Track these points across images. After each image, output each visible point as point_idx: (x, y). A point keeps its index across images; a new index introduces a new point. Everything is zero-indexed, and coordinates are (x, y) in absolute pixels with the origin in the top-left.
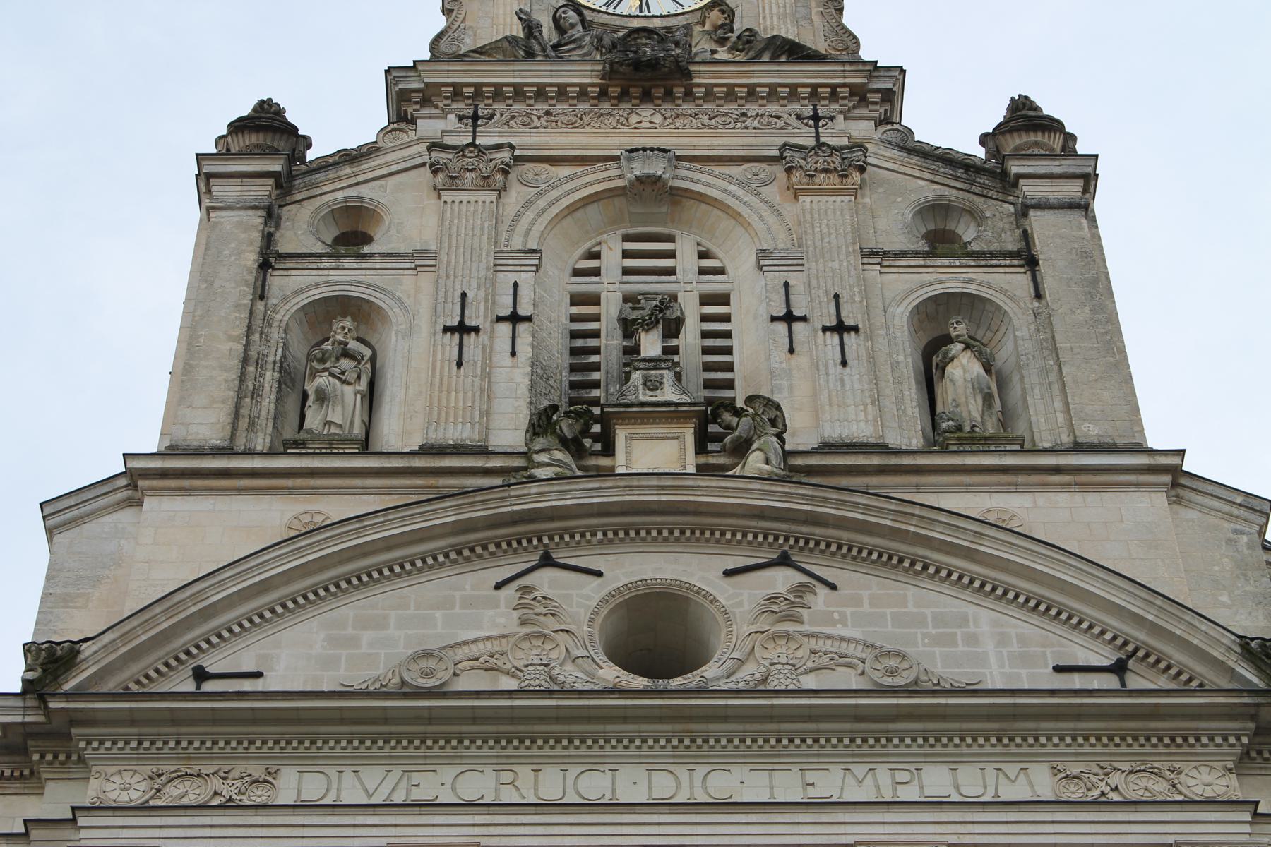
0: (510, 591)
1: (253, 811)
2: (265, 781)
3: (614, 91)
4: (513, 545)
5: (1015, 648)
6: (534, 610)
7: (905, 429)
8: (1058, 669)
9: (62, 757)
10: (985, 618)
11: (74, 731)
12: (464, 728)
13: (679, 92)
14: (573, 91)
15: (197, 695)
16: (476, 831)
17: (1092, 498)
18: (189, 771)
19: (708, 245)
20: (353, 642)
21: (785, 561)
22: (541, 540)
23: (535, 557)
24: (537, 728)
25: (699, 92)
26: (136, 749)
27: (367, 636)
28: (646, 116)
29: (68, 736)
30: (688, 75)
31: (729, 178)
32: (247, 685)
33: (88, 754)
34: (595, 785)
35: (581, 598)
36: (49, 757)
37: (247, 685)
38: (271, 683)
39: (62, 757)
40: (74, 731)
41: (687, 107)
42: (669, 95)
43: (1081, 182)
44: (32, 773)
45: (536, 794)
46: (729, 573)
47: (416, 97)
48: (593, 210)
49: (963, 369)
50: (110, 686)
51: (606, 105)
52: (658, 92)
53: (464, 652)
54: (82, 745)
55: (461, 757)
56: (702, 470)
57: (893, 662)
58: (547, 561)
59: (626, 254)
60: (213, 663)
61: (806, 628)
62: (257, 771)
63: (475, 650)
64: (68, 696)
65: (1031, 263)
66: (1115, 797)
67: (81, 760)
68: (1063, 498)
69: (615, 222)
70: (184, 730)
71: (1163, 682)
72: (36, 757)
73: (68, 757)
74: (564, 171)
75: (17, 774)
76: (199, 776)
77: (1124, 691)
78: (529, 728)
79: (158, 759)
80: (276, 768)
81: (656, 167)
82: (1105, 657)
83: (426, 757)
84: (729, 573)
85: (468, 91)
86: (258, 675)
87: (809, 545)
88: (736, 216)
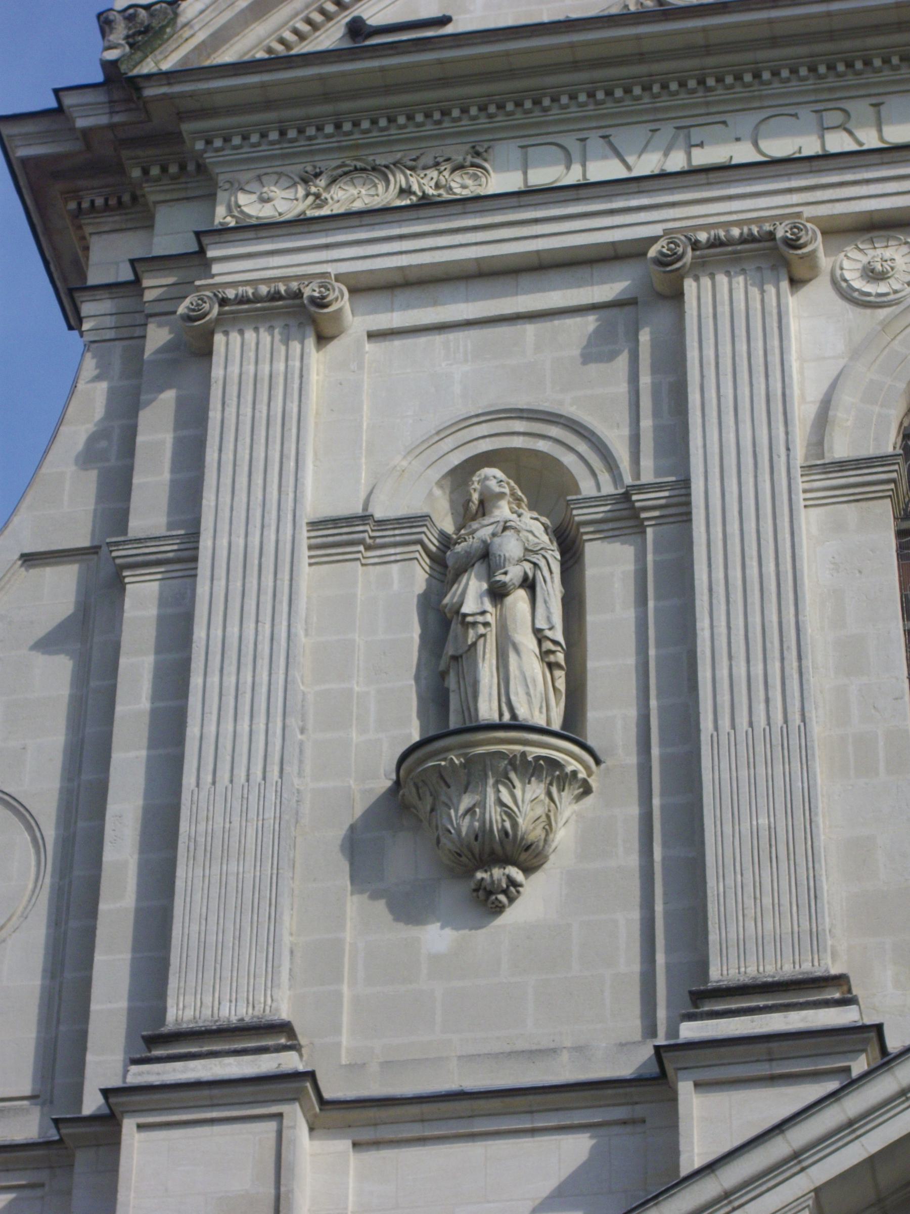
1: (458, 208)
2: (473, 165)
9: (173, 169)
11: (187, 127)
12: (761, 55)
16: (795, 198)
18: (359, 164)
24: (871, 42)
26: (278, 142)
29: (175, 138)
33: (210, 158)
36: (155, 171)
38: (461, 25)
39: (173, 169)
40: (187, 127)
44: (134, 199)
45: (882, 139)
50: (228, 55)
54: (200, 145)
55: (761, 98)
64: (168, 77)
67: (201, 168)
70: (345, 106)
72: (136, 173)
73: (183, 167)
75: (113, 202)
76: (374, 169)
78: (857, 43)
79: (311, 153)
80: (486, 145)
83: (707, 104)
86: (445, 20)
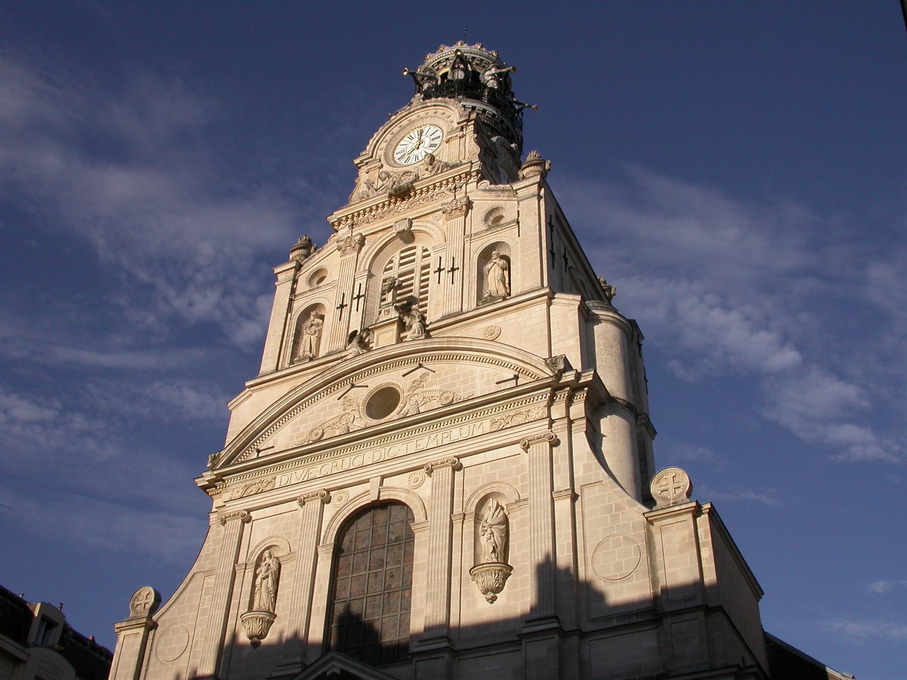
0: (342, 399)
5: (486, 379)
7: (470, 303)
8: (498, 383)
10: (478, 369)
13: (412, 194)
15: (258, 458)
17: (522, 312)
19: (426, 247)
20: (298, 429)
21: (421, 366)
25: (418, 192)
27: (303, 425)
30: (414, 188)
31: (427, 222)
32: (270, 452)
34: (358, 461)
37: (270, 452)
42: (410, 197)
46: (404, 376)
47: (336, 224)
49: (494, 271)
53: (326, 425)
57: (445, 395)
58: (353, 386)
60: (261, 447)
61: (425, 389)
62: (270, 478)
63: (328, 424)
65: (518, 223)
66: (507, 426)
68: (513, 315)
71: (529, 379)
74: (380, 234)
77: (517, 386)
82: (510, 374)
84: (404, 376)
85: (350, 216)
87: (427, 359)
88: (429, 234)
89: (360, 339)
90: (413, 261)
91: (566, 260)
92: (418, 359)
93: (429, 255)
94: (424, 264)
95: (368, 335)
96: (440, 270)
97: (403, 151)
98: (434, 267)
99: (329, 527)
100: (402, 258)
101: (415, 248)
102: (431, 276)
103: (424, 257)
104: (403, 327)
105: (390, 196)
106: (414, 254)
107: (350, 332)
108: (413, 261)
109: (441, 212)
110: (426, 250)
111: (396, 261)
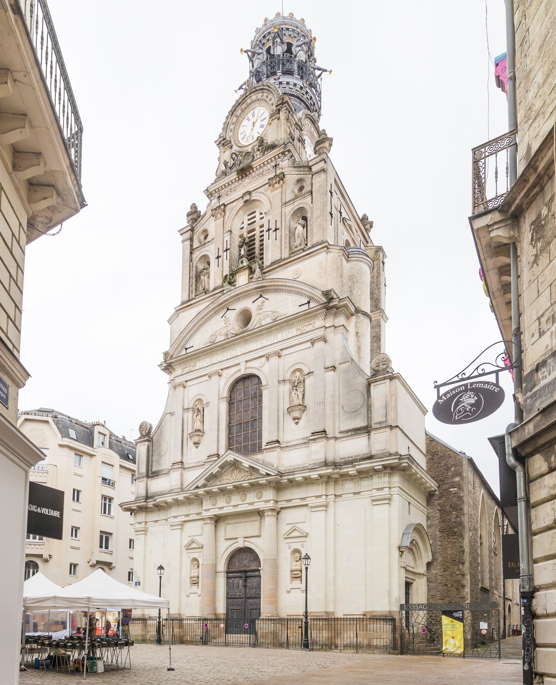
3: (240, 177)
4: (222, 308)
6: (227, 321)
13: (251, 171)
14: (233, 181)
22: (226, 306)
23: (226, 309)
28: (247, 180)
35: (232, 315)
41: (254, 174)
43: (323, 161)
48: (241, 212)
51: (240, 181)
52: (248, 173)
56: (249, 283)
58: (228, 309)
59: (249, 220)
69: (245, 213)
81: (247, 198)
89: (230, 279)
90: (255, 222)
91: (341, 213)
92: (262, 291)
93: (263, 218)
94: (261, 224)
95: (233, 277)
96: (269, 230)
97: (244, 132)
98: (265, 228)
99: (224, 388)
100: (249, 220)
101: (254, 212)
102: (264, 233)
103: (261, 219)
104: (252, 272)
105: (238, 174)
106: (255, 217)
107: (224, 275)
108: (255, 222)
109: (268, 185)
110: (261, 214)
111: (246, 222)
